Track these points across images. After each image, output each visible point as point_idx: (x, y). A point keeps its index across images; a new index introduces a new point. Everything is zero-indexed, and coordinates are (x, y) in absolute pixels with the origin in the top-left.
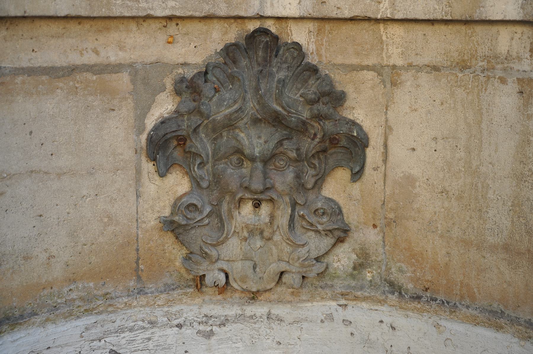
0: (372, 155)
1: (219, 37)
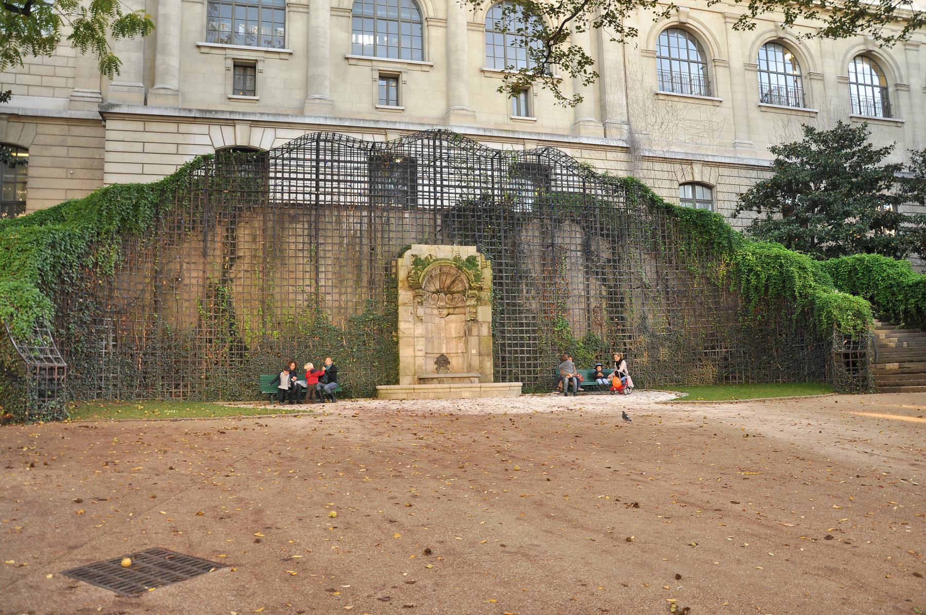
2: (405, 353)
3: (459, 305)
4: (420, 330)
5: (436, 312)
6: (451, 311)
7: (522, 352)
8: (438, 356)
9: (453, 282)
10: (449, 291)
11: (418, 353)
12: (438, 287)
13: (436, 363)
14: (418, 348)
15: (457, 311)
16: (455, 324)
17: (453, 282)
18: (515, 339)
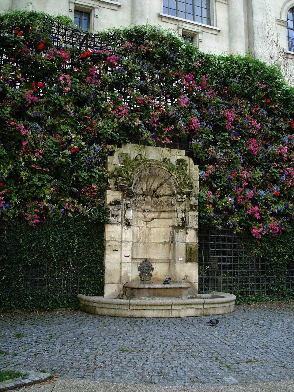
0: (154, 269)
1: (143, 261)
2: (111, 260)
3: (167, 209)
4: (128, 234)
5: (141, 215)
6: (156, 215)
7: (224, 260)
8: (141, 261)
9: (161, 185)
10: (154, 193)
11: (125, 259)
12: (144, 190)
13: (139, 269)
14: (124, 253)
15: (163, 215)
16: (159, 229)
17: (161, 185)
18: (218, 246)
